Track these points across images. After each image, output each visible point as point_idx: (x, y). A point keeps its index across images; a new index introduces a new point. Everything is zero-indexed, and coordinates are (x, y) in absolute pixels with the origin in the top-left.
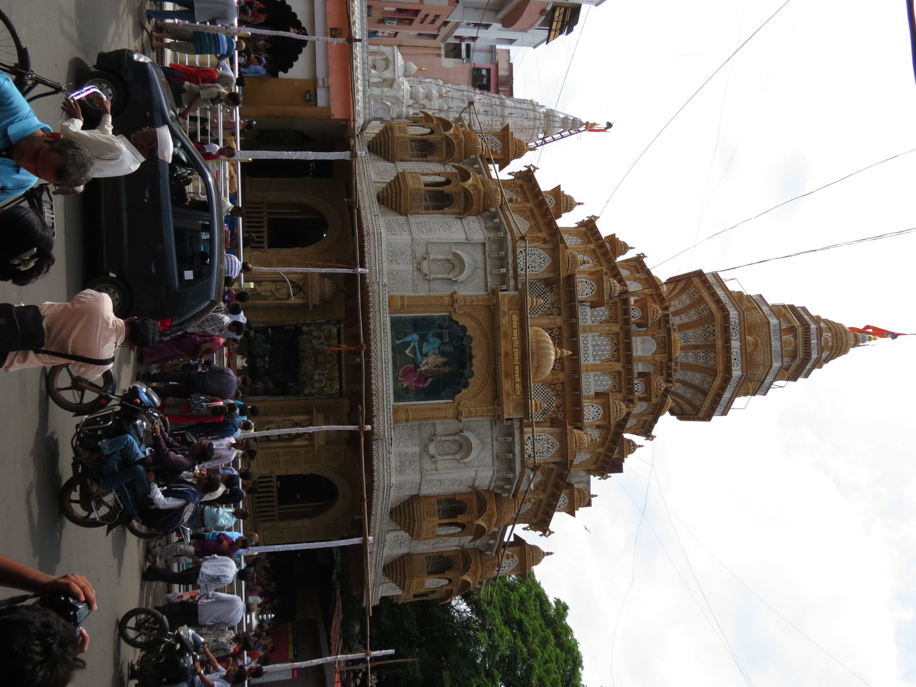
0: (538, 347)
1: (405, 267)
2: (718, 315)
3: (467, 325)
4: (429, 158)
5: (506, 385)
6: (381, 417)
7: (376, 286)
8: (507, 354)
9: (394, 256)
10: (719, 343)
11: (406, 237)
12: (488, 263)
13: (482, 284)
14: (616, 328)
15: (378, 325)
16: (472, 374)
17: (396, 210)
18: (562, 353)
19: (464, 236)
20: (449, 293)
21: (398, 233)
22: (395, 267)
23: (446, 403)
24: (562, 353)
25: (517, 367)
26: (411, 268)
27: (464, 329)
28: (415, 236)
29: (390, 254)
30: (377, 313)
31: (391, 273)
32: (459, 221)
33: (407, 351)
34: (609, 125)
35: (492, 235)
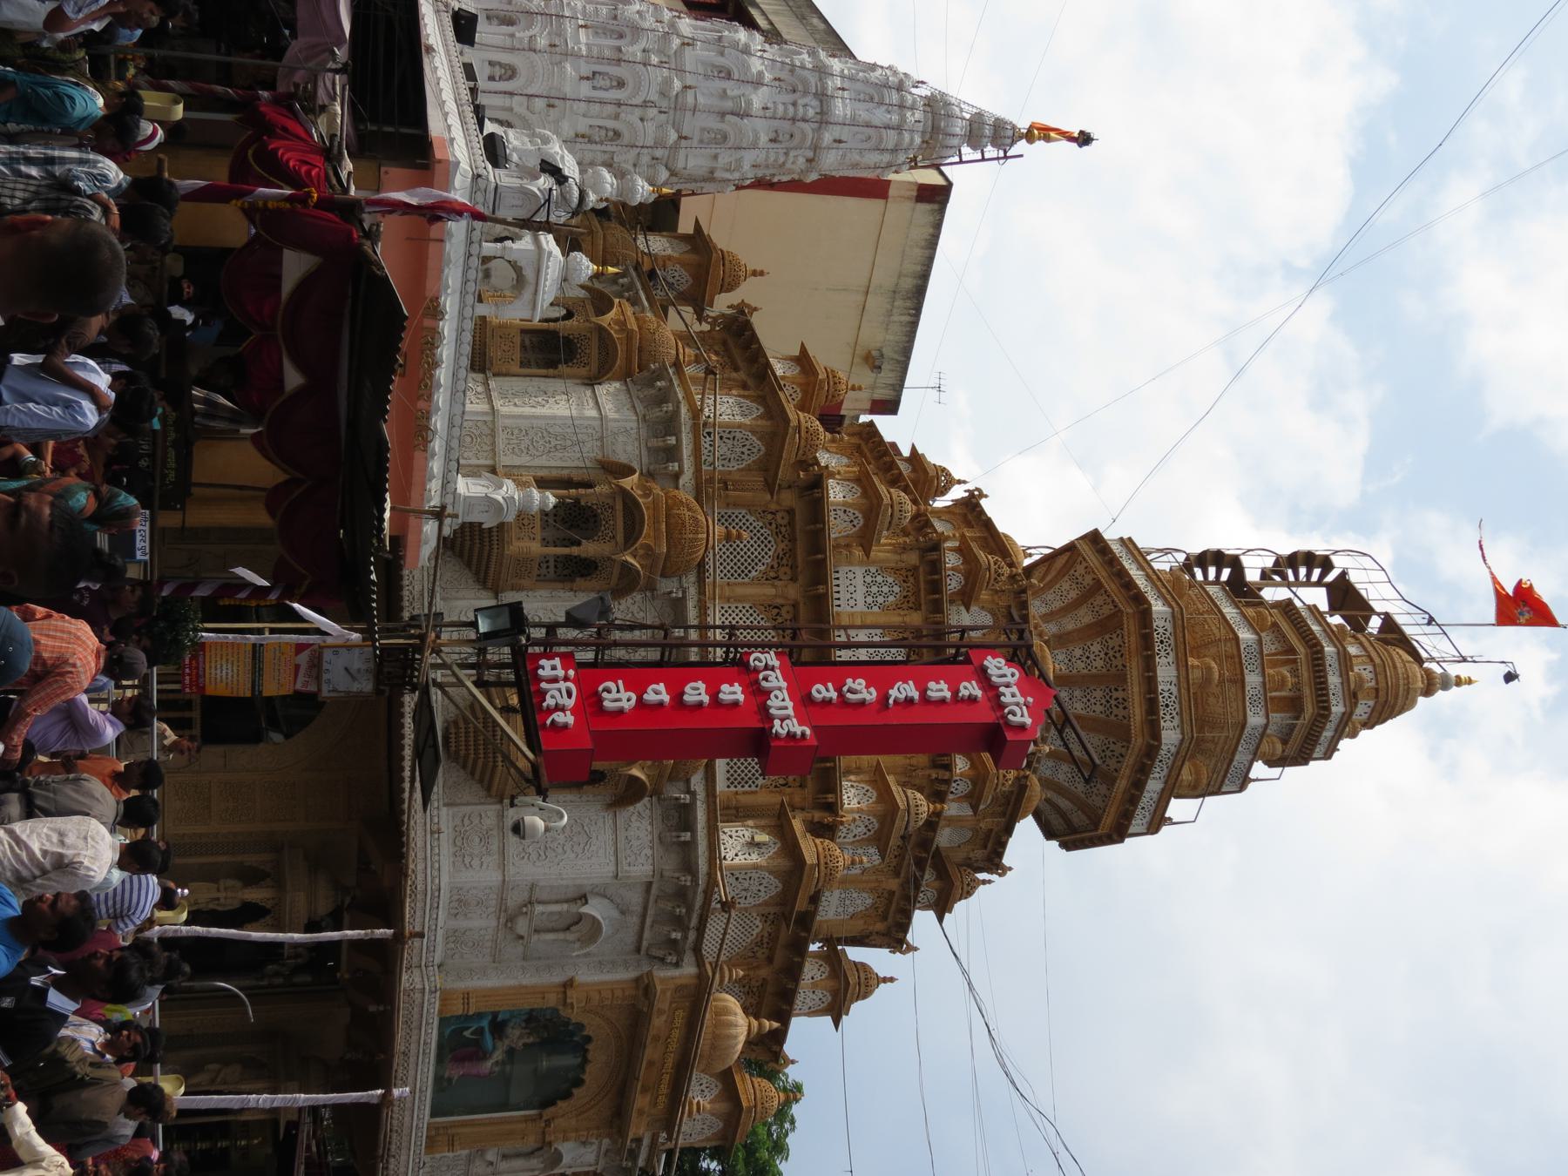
0: (713, 1047)
1: (482, 923)
2: (1138, 741)
3: (585, 1022)
4: (579, 582)
5: (641, 1101)
6: (403, 1158)
7: (418, 995)
8: (651, 1064)
9: (461, 904)
10: (1122, 784)
11: (492, 877)
12: (651, 912)
13: (630, 938)
14: (893, 884)
15: (413, 1047)
16: (579, 1082)
17: (481, 781)
18: (760, 1025)
19: (612, 868)
20: (558, 978)
21: (476, 863)
22: (462, 923)
23: (526, 1119)
24: (760, 1025)
25: (667, 1077)
26: (494, 923)
27: (581, 1026)
28: (511, 870)
29: (455, 904)
30: (415, 1032)
31: (454, 937)
32: (609, 817)
33: (467, 1034)
34: (1084, 139)
35: (670, 864)
